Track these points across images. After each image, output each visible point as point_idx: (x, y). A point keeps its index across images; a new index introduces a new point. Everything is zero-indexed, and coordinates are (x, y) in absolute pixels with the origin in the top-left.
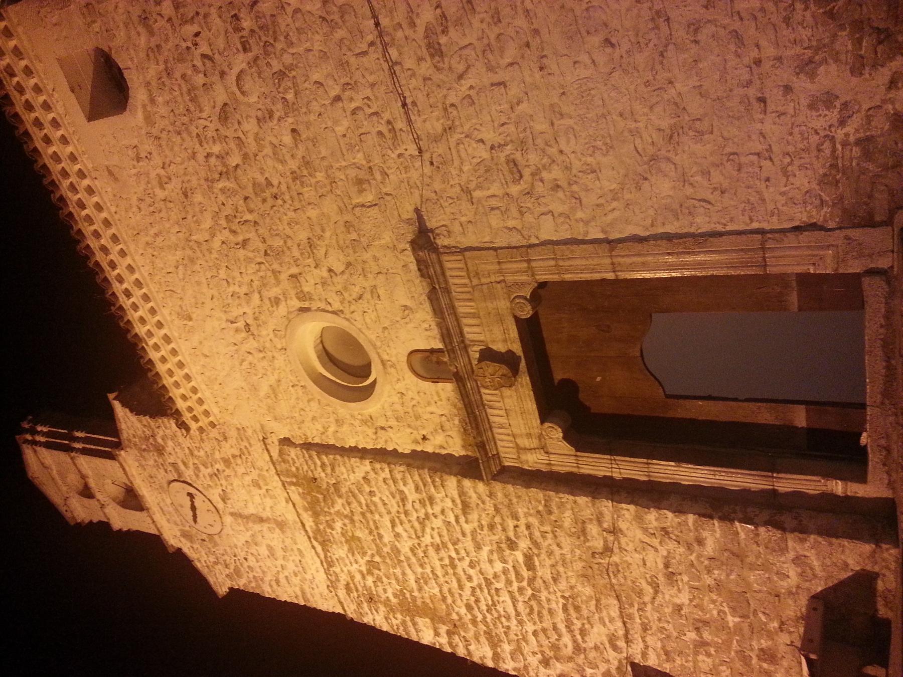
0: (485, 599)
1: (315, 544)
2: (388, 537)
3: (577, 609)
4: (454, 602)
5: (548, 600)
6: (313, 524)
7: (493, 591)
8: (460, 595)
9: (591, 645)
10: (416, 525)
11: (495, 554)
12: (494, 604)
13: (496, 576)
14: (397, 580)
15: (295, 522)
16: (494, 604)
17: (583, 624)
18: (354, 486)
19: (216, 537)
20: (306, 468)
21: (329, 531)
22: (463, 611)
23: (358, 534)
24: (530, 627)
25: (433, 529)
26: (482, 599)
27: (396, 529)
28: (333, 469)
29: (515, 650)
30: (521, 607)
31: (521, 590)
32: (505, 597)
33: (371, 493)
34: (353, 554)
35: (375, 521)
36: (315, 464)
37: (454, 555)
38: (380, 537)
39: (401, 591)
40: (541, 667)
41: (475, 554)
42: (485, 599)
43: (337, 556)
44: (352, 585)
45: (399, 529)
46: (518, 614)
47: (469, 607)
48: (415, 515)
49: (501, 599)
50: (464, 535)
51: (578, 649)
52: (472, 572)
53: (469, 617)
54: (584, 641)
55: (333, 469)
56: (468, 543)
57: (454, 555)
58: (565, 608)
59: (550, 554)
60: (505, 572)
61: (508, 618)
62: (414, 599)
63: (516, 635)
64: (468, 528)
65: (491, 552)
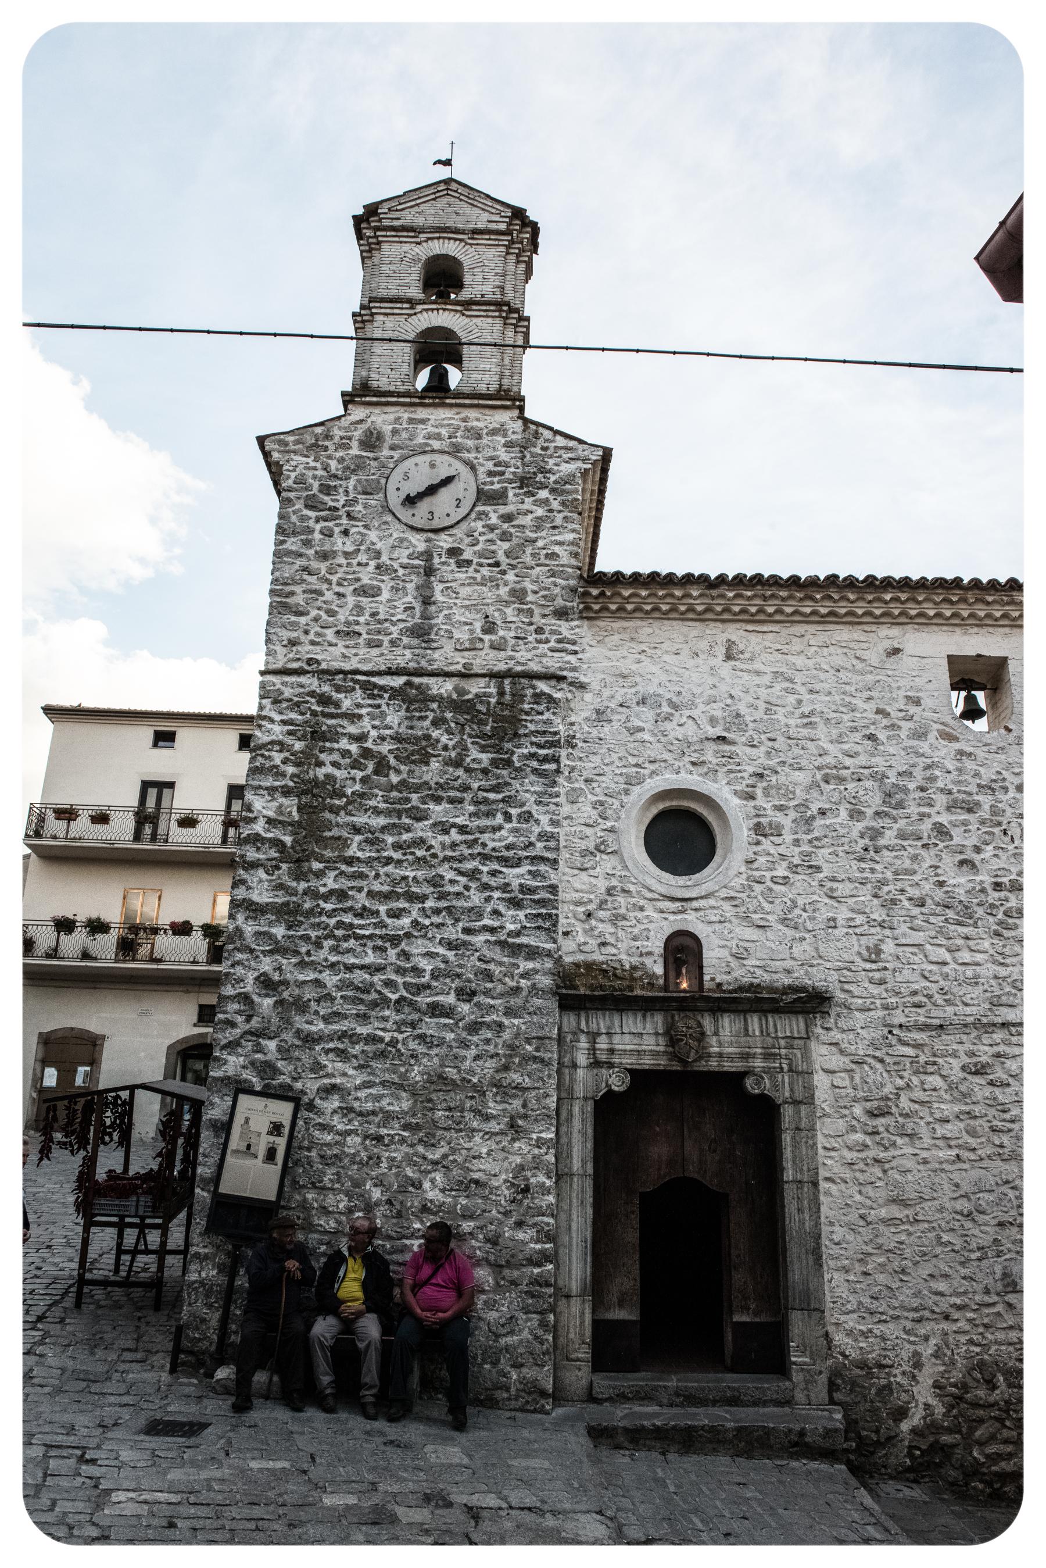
0: (361, 927)
1: (401, 681)
2: (438, 811)
3: (382, 1055)
4: (342, 873)
5: (385, 1019)
6: (435, 692)
7: (379, 943)
8: (360, 890)
9: (323, 1060)
10: (470, 865)
11: (442, 966)
12: (357, 937)
13: (406, 955)
14: (362, 795)
15: (430, 662)
16: (357, 937)
17: (355, 1057)
18: (513, 793)
19: (381, 496)
20: (532, 727)
21: (431, 715)
22: (330, 882)
23: (435, 765)
24: (330, 979)
25: (467, 888)
26: (362, 922)
27: (453, 831)
28: (535, 771)
29: (277, 942)
30: (359, 977)
31: (389, 983)
32: (371, 958)
33: (508, 817)
34: (392, 738)
35: (461, 801)
36: (540, 746)
37: (429, 904)
38: (438, 800)
39: (344, 795)
40: (256, 974)
41: (439, 937)
42: (361, 927)
43: (384, 707)
44: (332, 710)
45: (455, 835)
46: (350, 968)
47: (342, 895)
48: (485, 869)
49: (370, 952)
50: (467, 931)
51: (309, 1040)
52: (406, 921)
53: (322, 890)
54: (327, 1052)
55: (535, 771)
56: (453, 933)
57: (429, 904)
58: (372, 1039)
59: (464, 1044)
60: (417, 971)
61: (335, 949)
62: (335, 810)
63: (308, 953)
64: (479, 939)
65: (446, 962)
